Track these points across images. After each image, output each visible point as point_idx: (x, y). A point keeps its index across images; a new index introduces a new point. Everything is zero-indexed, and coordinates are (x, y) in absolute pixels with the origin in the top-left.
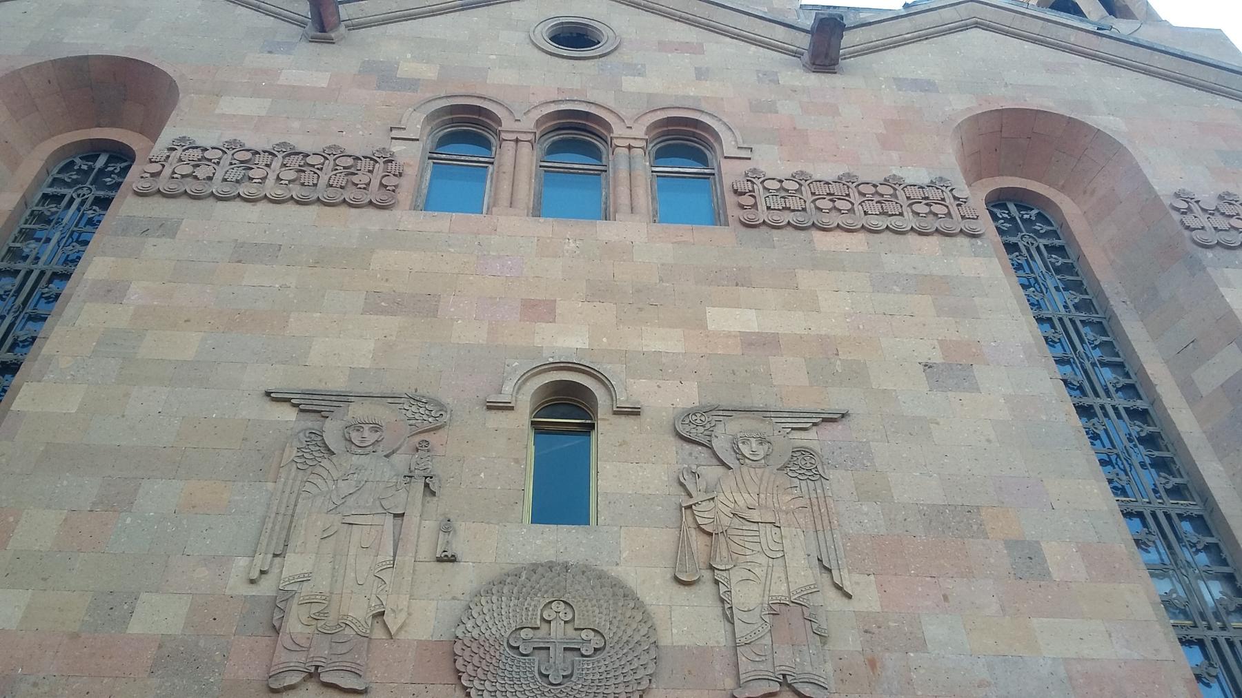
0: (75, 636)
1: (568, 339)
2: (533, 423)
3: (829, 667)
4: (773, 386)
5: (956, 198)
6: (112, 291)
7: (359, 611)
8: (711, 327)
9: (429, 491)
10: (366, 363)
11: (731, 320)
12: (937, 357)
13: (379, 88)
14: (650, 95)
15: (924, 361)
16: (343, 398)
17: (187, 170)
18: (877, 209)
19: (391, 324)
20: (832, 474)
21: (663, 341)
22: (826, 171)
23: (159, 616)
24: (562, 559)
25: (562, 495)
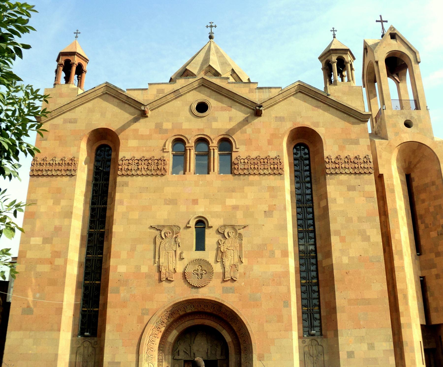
0: (134, 273)
1: (200, 210)
2: (195, 227)
3: (238, 275)
4: (236, 218)
5: (280, 162)
6: (121, 203)
7: (171, 268)
8: (227, 204)
9: (179, 246)
10: (166, 218)
11: (231, 202)
12: (267, 209)
13: (160, 134)
14: (218, 129)
15: (265, 210)
16: (164, 226)
17: (126, 167)
18: (262, 167)
19: (170, 207)
20: (244, 239)
21: (217, 208)
22: (254, 155)
23: (144, 269)
24: (200, 258)
25: (200, 245)
